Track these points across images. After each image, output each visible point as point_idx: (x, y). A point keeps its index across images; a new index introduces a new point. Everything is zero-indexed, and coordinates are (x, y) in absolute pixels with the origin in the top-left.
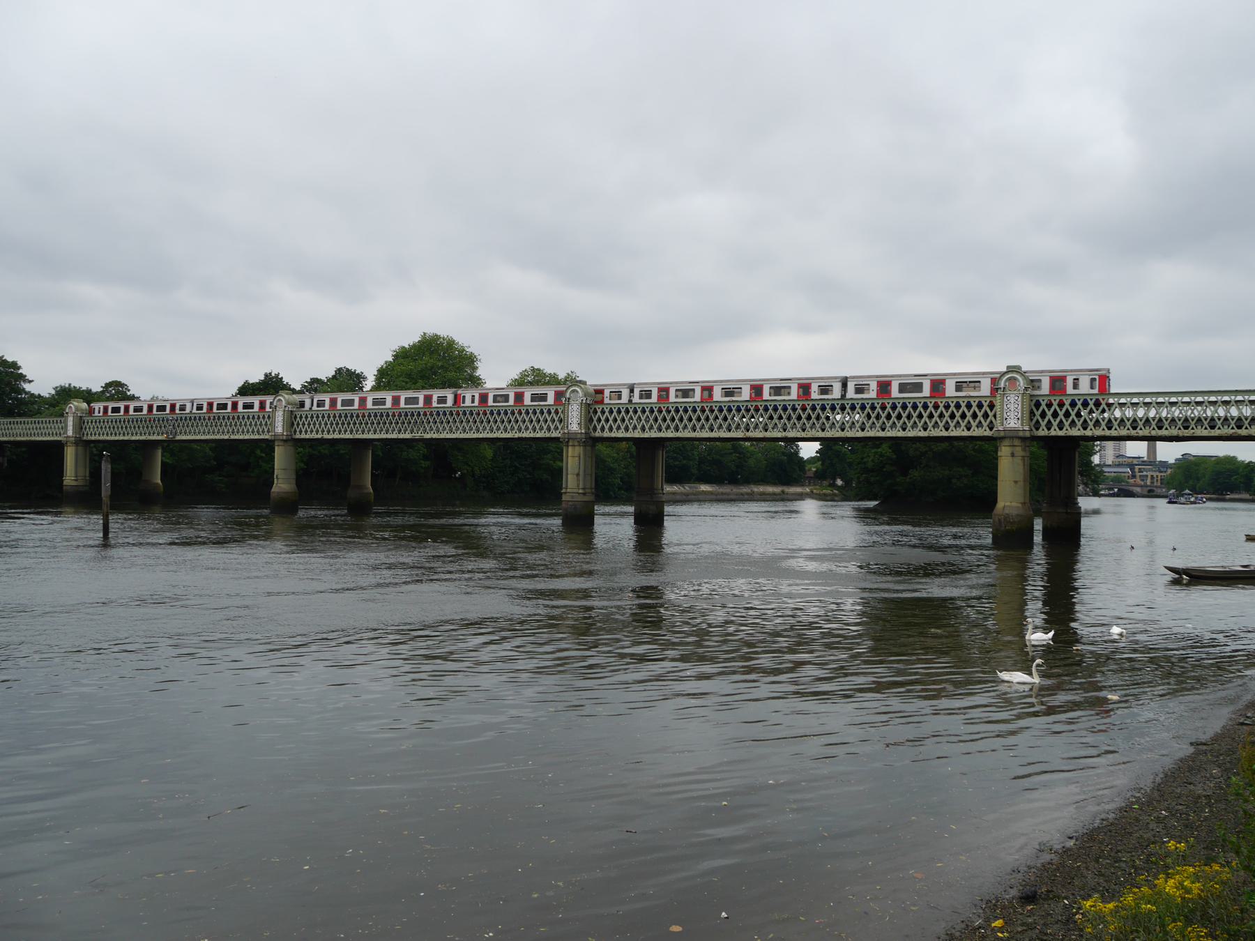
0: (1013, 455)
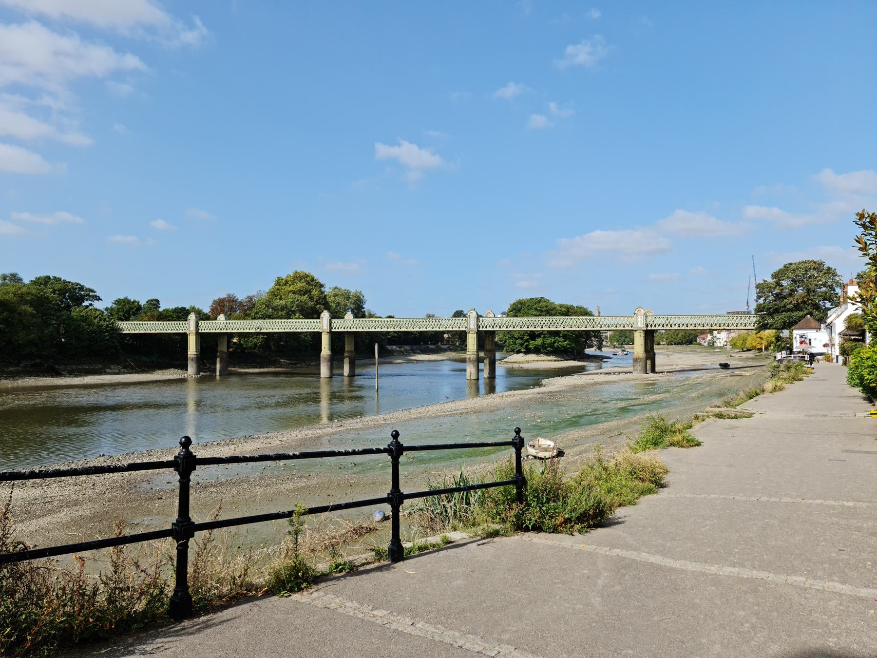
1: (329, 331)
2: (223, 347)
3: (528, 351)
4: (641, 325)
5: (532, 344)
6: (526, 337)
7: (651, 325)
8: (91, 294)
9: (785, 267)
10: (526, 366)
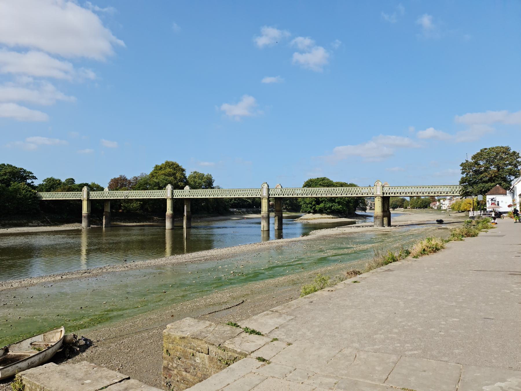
0: (379, 201)
1: (171, 198)
2: (108, 209)
3: (315, 212)
4: (379, 192)
5: (318, 207)
6: (313, 203)
7: (387, 193)
8: (30, 175)
9: (481, 151)
10: (311, 222)
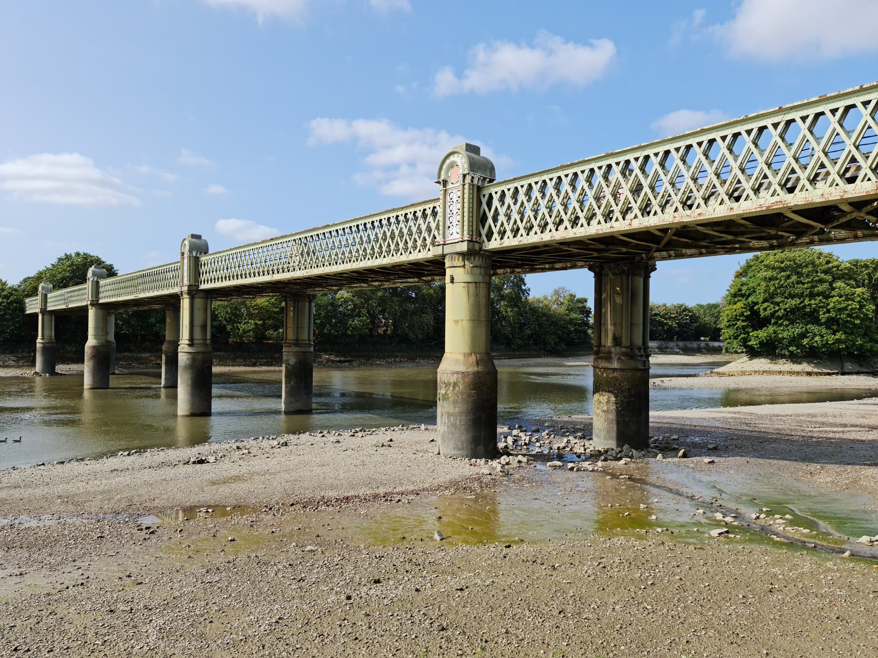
6: (740, 324)
